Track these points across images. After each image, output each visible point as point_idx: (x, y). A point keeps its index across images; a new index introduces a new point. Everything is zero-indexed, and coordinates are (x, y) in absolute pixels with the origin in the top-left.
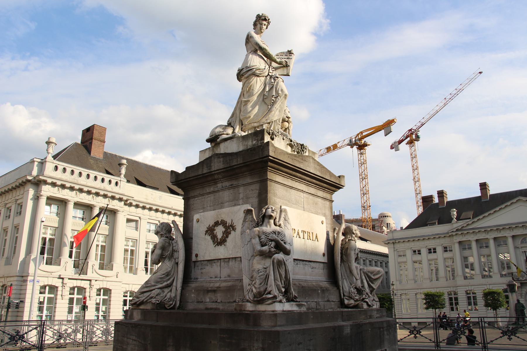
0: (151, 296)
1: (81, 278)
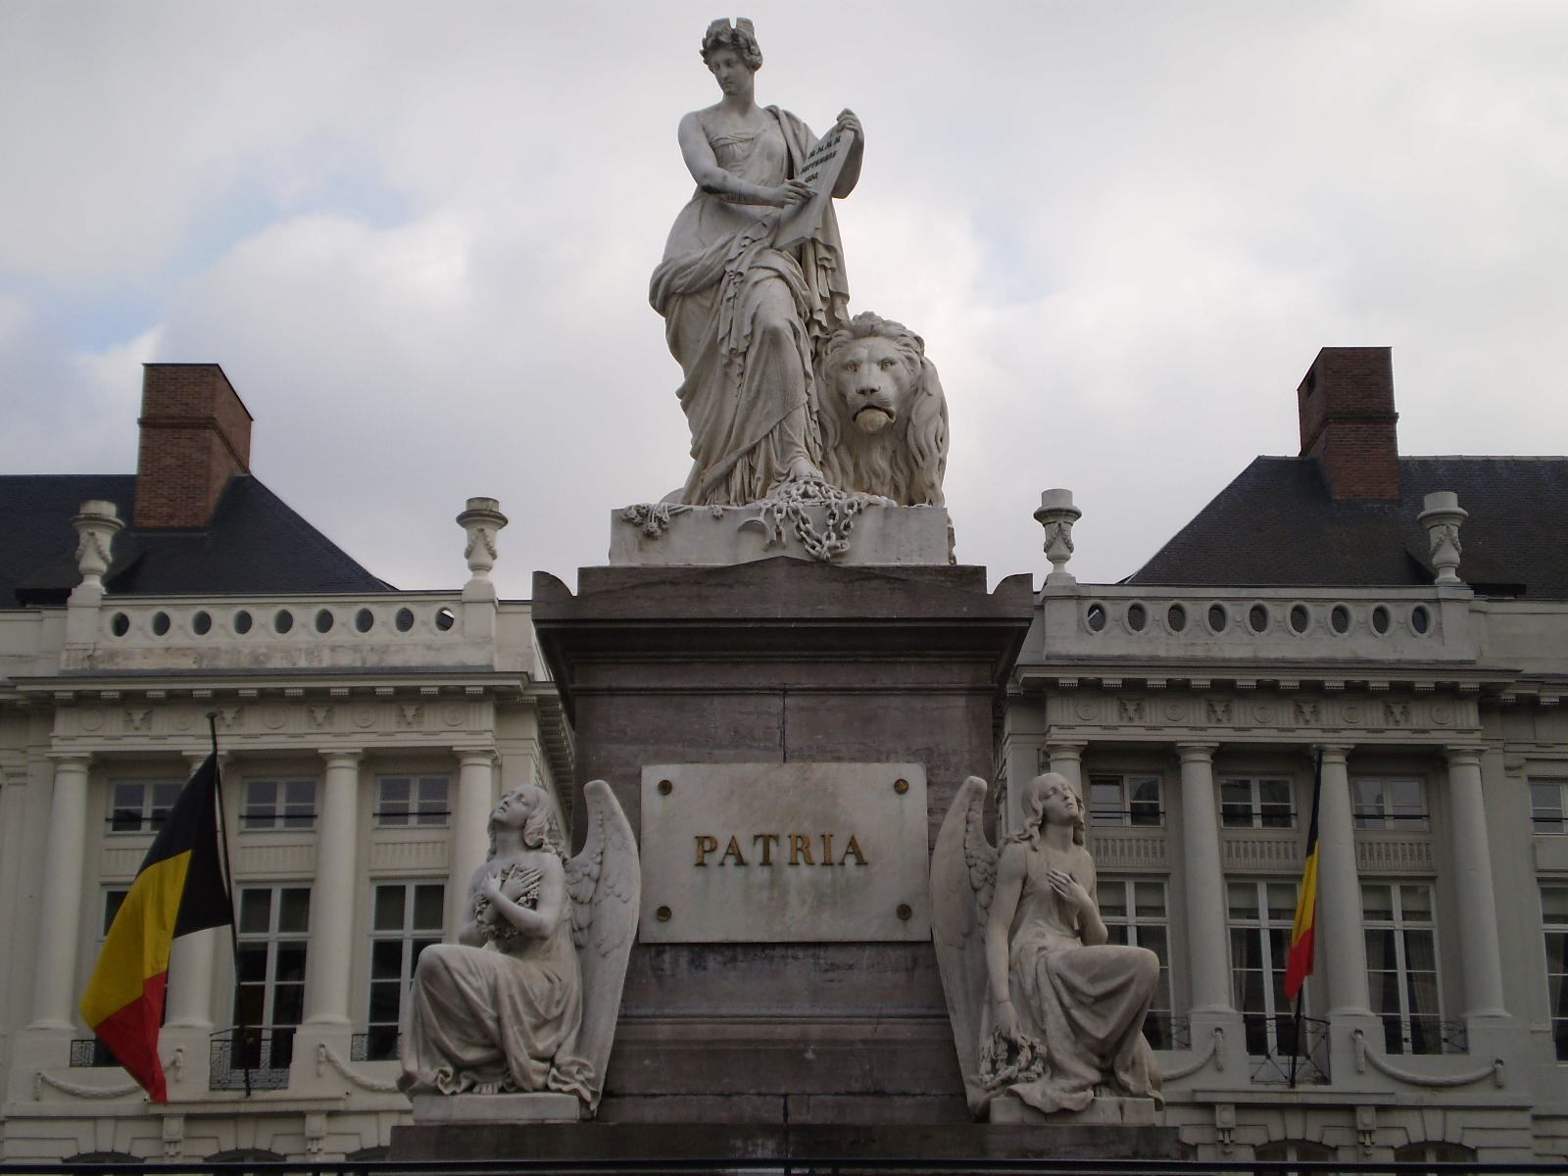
1: (1295, 1099)
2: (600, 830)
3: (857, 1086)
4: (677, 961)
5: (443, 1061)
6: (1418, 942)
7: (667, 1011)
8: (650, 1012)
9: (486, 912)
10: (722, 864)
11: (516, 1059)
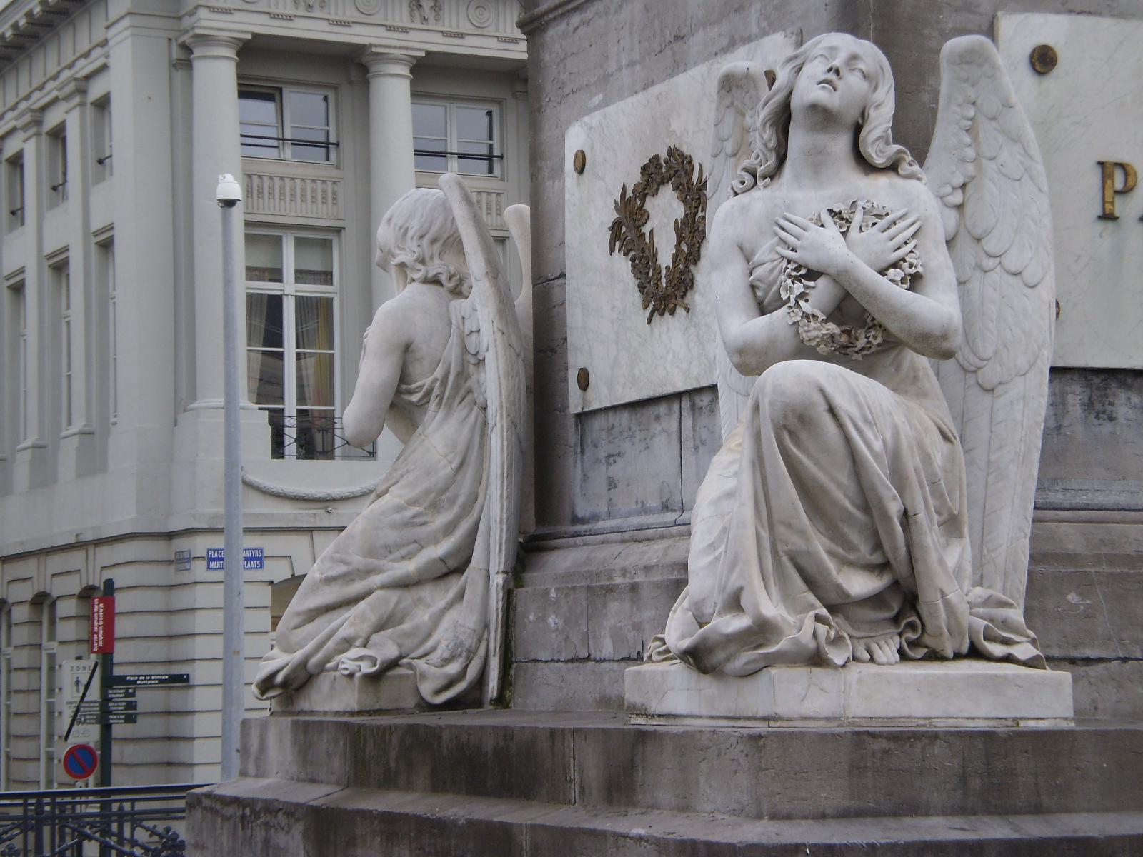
0: (341, 634)
2: (968, 139)
4: (1064, 403)
5: (811, 597)
6: (316, 314)
9: (813, 295)
11: (943, 595)
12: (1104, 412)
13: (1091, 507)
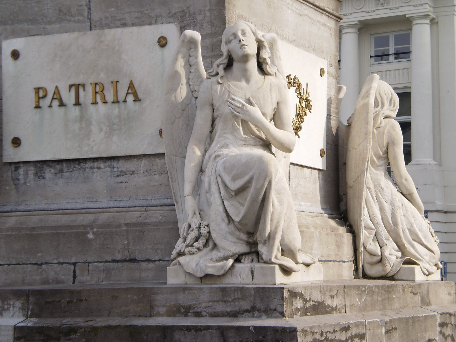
3: (119, 257)
4: (27, 174)
7: (22, 208)
8: (9, 209)
10: (50, 106)
12: (41, 176)
13: (31, 210)
